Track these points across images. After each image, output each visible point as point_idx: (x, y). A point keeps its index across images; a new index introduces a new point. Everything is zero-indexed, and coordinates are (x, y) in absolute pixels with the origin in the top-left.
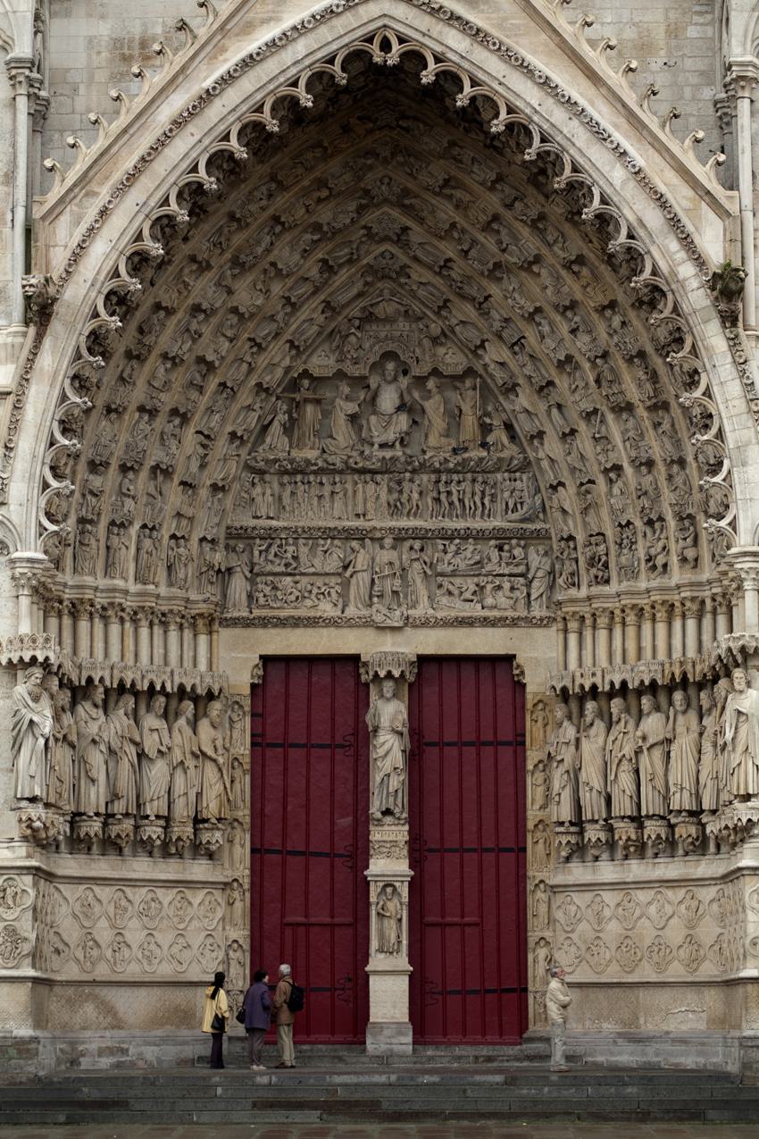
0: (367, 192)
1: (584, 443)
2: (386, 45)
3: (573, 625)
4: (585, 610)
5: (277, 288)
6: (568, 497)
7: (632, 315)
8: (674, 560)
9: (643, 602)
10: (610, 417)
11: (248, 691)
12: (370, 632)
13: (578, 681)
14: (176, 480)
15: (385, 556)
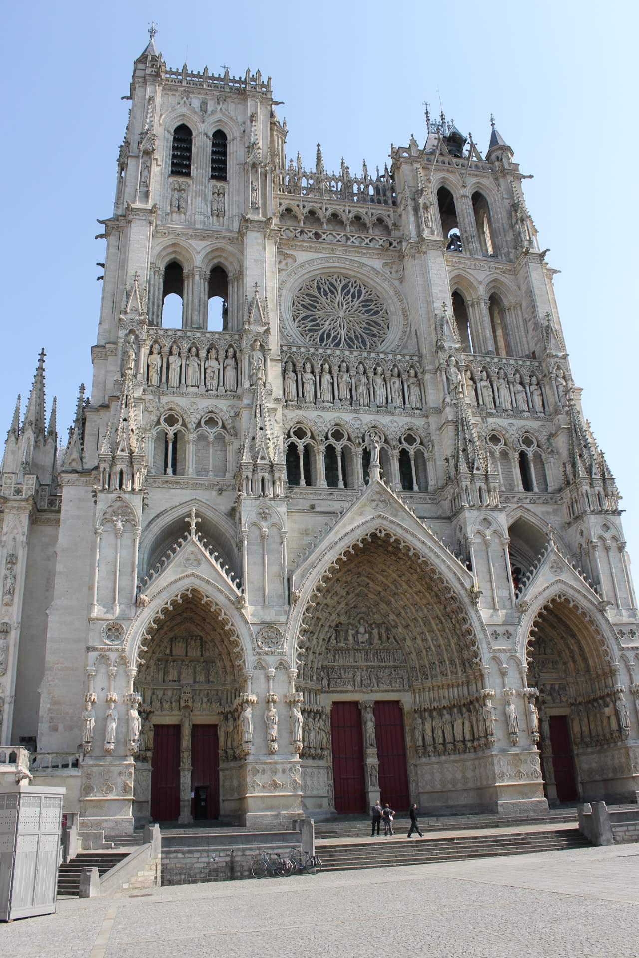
0: (359, 573)
1: (419, 641)
2: (380, 531)
3: (417, 691)
4: (420, 687)
5: (336, 599)
6: (414, 656)
7: (435, 605)
8: (449, 671)
9: (440, 684)
10: (427, 634)
11: (329, 711)
12: (362, 694)
13: (423, 706)
14: (311, 651)
15: (364, 673)
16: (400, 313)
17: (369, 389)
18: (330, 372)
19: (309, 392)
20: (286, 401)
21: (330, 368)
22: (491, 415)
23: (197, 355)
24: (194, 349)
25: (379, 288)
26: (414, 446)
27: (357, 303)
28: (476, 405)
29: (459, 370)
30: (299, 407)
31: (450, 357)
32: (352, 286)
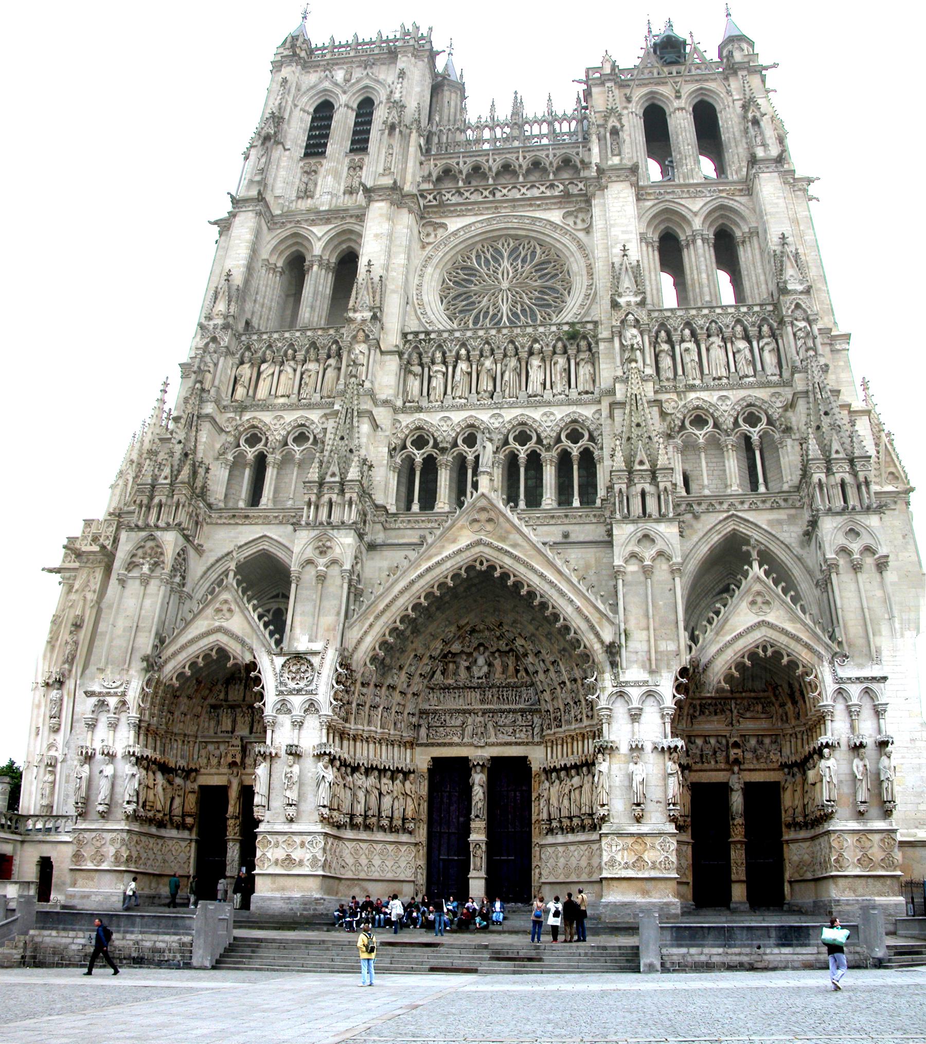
16: (584, 272)
17: (520, 375)
18: (468, 359)
19: (434, 388)
20: (404, 403)
21: (468, 352)
22: (692, 388)
23: (294, 358)
24: (290, 352)
25: (558, 245)
26: (579, 444)
27: (527, 267)
28: (671, 376)
29: (641, 333)
30: (420, 409)
31: (627, 315)
32: (524, 248)
